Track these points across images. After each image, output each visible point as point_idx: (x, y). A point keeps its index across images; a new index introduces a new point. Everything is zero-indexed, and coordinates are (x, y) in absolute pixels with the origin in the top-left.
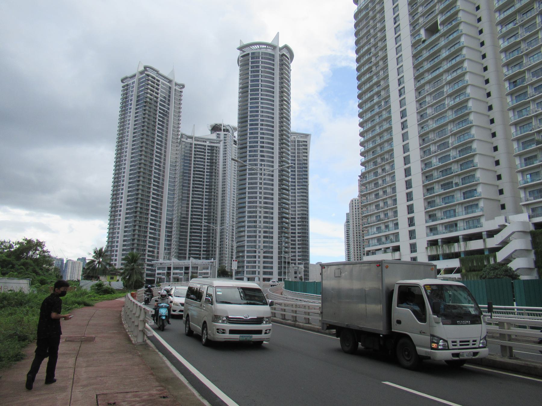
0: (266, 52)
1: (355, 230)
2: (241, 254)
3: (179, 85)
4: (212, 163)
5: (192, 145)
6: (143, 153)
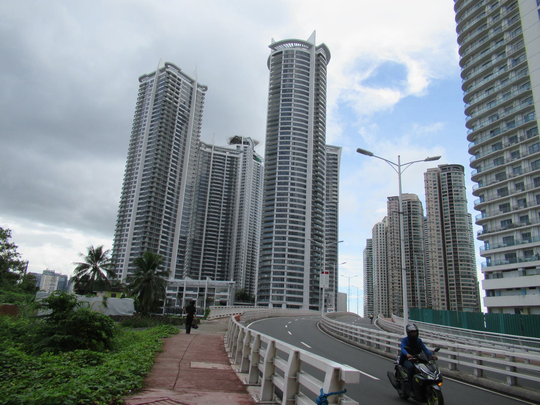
0: (301, 50)
2: (266, 276)
3: (202, 87)
4: (232, 175)
5: (211, 155)
6: (159, 156)
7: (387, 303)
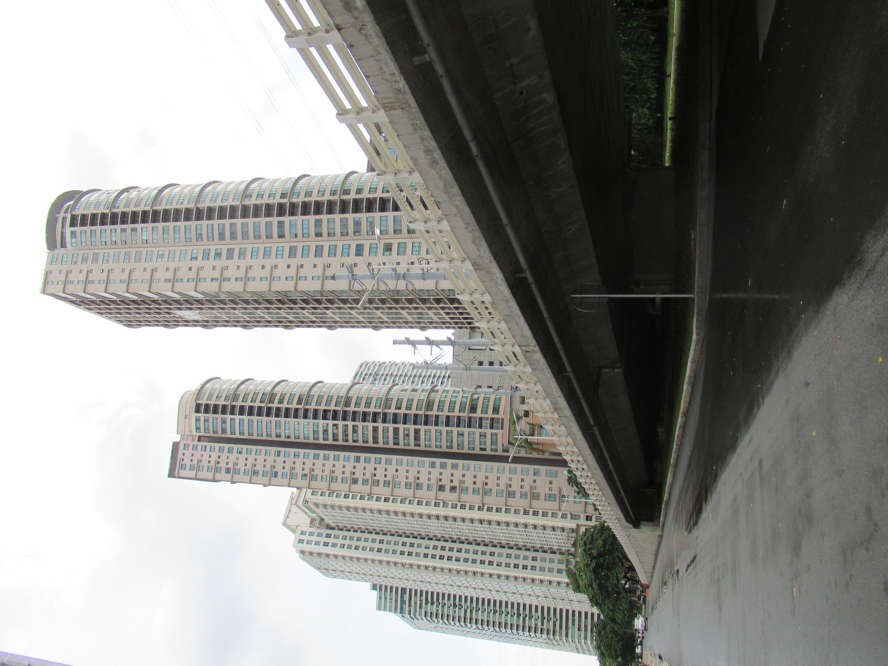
1: (392, 558)
7: (531, 554)
